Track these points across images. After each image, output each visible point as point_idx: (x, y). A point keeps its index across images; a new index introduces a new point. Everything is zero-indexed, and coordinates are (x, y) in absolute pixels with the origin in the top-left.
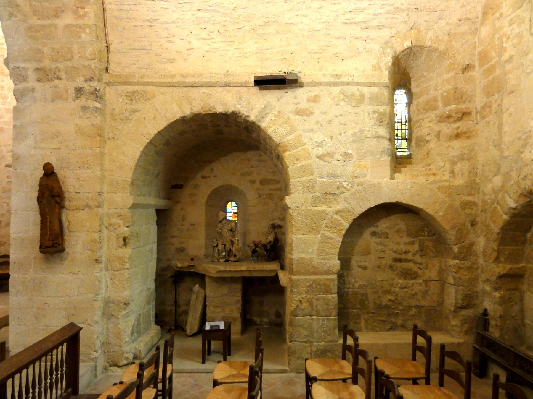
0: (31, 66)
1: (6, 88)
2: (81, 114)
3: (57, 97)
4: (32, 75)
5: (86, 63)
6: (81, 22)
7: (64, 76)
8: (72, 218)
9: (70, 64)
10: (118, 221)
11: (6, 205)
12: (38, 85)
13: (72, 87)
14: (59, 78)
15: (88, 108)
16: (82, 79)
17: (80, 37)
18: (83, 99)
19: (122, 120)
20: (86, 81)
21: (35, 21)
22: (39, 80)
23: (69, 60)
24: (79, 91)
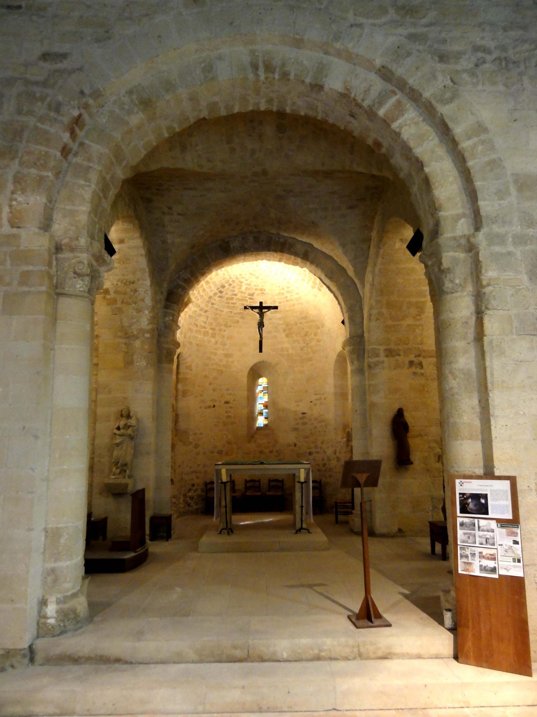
0: (382, 348)
1: (226, 337)
2: (413, 377)
3: (398, 366)
4: (382, 353)
5: (417, 346)
6: (417, 323)
7: (402, 353)
8: (413, 442)
9: (406, 346)
10: (435, 445)
11: (225, 436)
12: (386, 359)
13: (407, 360)
14: (399, 355)
15: (417, 373)
16: (413, 356)
17: (415, 331)
18: (414, 368)
19: (432, 380)
20: (416, 357)
21: (390, 323)
22: (387, 356)
23: (407, 344)
24: (411, 363)
